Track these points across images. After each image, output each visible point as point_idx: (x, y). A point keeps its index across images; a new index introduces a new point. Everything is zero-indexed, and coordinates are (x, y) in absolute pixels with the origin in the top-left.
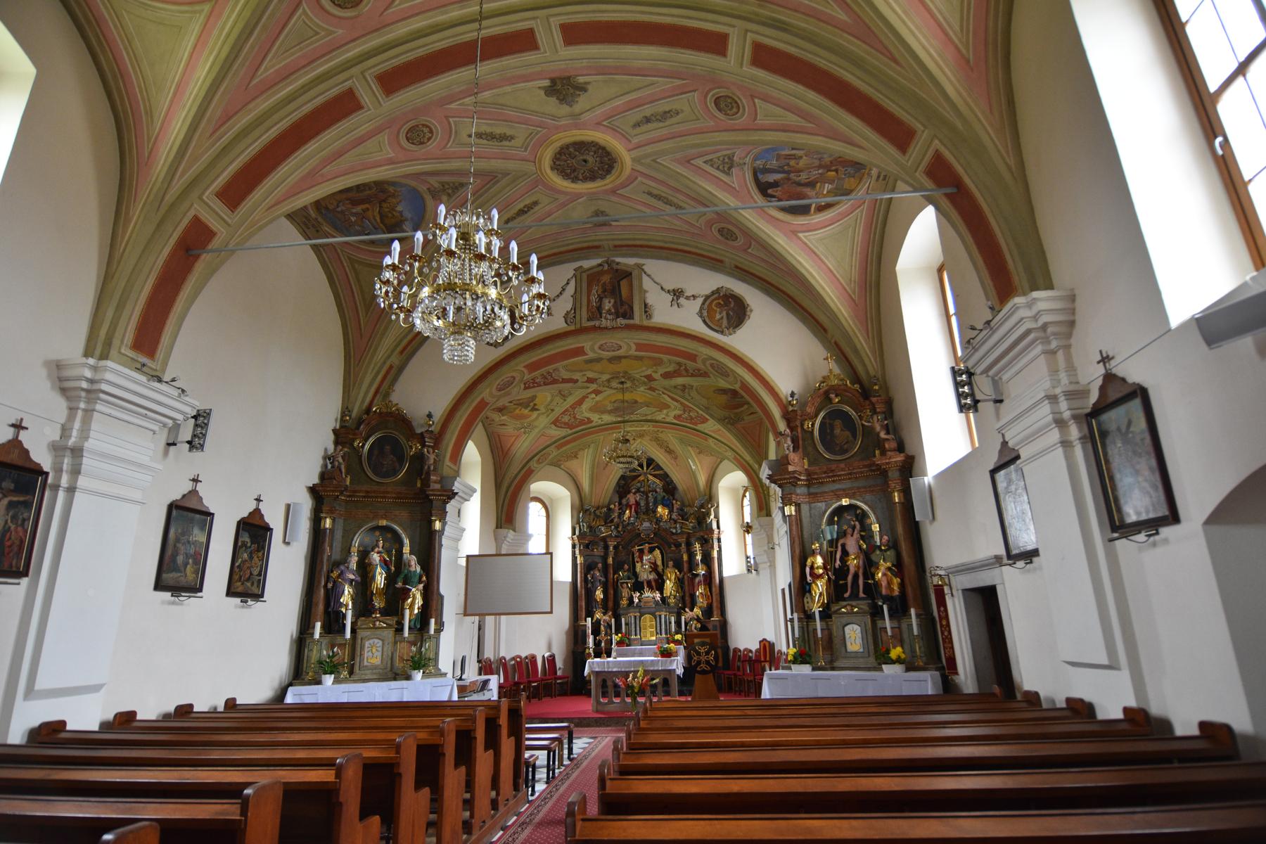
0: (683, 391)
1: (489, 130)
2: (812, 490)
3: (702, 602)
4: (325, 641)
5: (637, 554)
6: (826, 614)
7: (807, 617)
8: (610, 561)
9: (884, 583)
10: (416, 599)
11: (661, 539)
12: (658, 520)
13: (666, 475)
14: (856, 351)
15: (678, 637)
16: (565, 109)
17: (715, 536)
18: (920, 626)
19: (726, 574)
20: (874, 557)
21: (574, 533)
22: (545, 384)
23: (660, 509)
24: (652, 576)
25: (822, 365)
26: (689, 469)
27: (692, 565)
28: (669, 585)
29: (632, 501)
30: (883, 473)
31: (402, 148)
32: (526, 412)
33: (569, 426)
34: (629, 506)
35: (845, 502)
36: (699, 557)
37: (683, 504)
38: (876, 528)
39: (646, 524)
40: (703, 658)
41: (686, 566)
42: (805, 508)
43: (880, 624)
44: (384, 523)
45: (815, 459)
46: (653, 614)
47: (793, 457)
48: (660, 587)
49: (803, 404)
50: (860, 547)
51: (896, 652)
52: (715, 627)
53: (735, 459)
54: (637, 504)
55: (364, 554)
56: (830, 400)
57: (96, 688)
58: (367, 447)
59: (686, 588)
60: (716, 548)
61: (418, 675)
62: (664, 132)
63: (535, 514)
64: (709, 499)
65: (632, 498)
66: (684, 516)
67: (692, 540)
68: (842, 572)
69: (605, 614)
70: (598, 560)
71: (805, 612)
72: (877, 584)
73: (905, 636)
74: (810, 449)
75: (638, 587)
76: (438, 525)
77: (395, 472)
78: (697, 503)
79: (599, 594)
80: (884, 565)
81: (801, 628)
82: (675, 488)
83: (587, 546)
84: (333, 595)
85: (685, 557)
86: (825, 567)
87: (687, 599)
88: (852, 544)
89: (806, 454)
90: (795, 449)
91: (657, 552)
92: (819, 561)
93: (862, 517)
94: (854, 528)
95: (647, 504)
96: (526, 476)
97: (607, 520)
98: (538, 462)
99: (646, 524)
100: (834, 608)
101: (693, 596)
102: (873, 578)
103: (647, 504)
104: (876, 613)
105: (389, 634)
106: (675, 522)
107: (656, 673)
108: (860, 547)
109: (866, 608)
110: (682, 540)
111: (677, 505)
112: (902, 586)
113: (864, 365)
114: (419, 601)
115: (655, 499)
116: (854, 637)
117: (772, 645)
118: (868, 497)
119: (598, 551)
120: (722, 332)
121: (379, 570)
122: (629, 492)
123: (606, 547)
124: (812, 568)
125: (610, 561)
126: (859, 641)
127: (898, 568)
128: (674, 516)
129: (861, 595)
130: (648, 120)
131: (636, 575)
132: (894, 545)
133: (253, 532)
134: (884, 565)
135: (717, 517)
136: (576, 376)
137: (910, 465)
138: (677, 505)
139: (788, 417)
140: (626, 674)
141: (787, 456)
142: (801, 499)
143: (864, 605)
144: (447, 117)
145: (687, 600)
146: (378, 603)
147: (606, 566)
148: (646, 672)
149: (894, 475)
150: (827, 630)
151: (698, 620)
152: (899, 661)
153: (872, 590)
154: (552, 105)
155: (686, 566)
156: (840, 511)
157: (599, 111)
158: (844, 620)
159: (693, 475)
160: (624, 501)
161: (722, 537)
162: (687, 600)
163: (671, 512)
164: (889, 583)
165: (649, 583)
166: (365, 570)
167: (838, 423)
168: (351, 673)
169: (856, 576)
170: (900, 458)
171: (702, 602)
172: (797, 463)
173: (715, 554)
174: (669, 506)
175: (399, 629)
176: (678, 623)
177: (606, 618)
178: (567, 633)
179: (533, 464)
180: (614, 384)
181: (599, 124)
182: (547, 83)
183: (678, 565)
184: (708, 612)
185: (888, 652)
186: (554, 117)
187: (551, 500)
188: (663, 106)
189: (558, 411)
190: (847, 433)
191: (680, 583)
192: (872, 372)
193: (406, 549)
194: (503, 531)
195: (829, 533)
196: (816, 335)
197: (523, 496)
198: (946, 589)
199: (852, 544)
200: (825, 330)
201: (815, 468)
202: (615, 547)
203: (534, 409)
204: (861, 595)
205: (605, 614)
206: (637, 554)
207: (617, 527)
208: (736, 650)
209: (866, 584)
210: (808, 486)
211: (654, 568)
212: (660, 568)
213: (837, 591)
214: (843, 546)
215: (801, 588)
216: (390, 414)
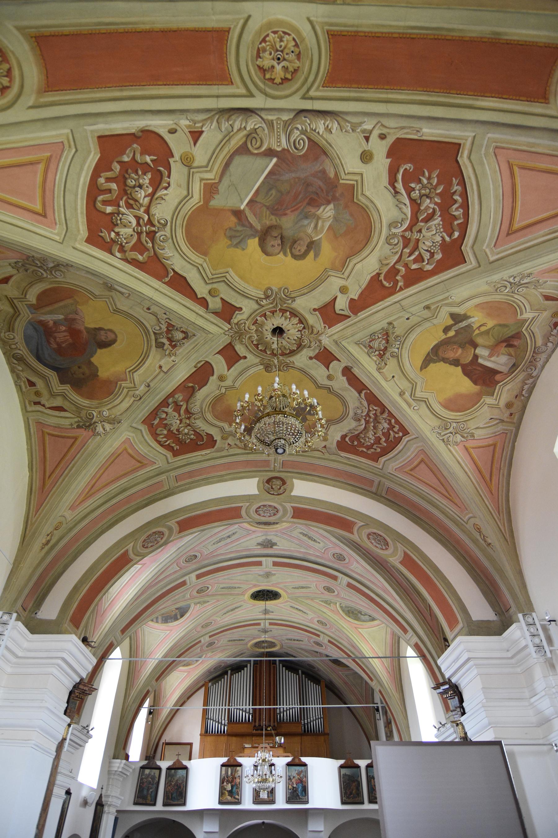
0: (170, 327)
1: (310, 541)
16: (269, 538)
22: (383, 408)
31: (349, 560)
32: (477, 319)
62: (220, 534)
130: (229, 537)
136: (341, 383)
144: (324, 553)
154: (275, 539)
157: (254, 536)
180: (292, 329)
181: (254, 532)
182: (274, 547)
186: (276, 535)
188: (220, 544)
203: (456, 318)
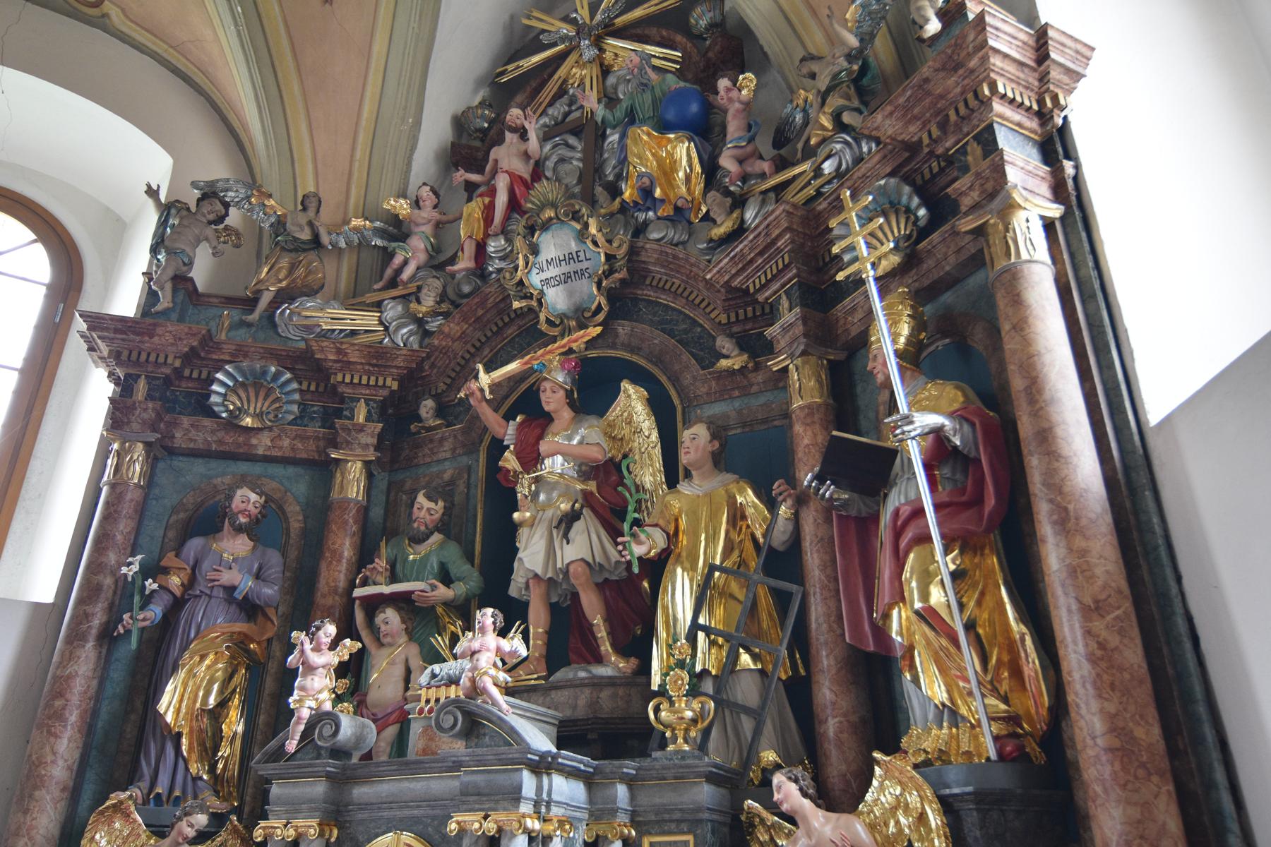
19: (1165, 381)
36: (890, 334)
60: (1032, 209)
87: (829, 693)
91: (632, 402)
101: (877, 673)
106: (739, 202)
122: (500, 140)
125: (352, 482)
147: (321, 510)
161: (1083, 112)
183: (755, 457)
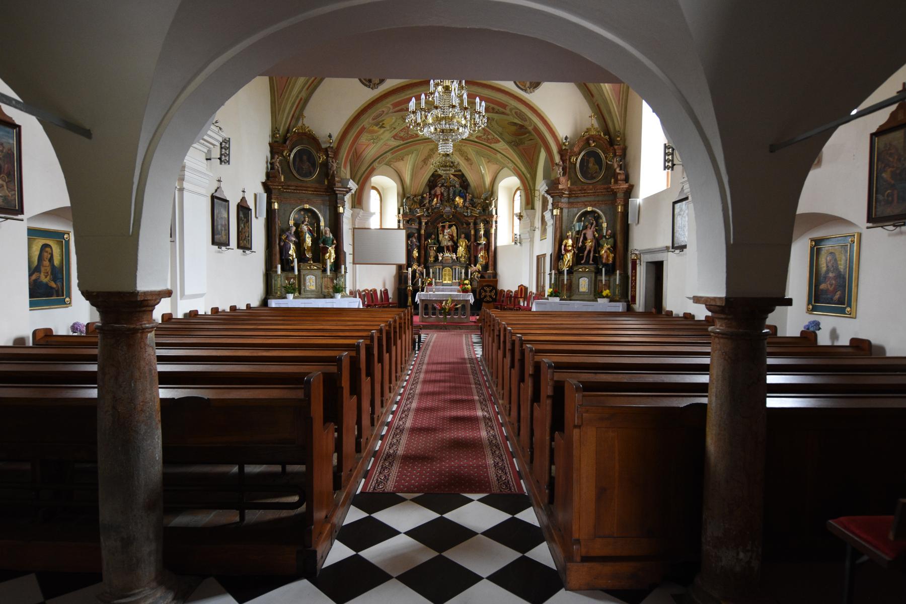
2: (571, 200)
3: (481, 261)
4: (284, 274)
5: (440, 229)
6: (570, 272)
7: (560, 273)
8: (423, 232)
9: (605, 256)
10: (331, 255)
11: (458, 219)
12: (456, 207)
13: (463, 175)
14: (610, 112)
15: (467, 282)
17: (494, 219)
18: (620, 279)
19: (498, 244)
20: (601, 242)
21: (399, 213)
23: (457, 199)
24: (450, 244)
25: (589, 120)
26: (480, 172)
27: (477, 237)
28: (461, 250)
29: (439, 192)
30: (614, 194)
32: (376, 128)
33: (402, 139)
34: (436, 196)
35: (589, 209)
36: (482, 232)
37: (473, 197)
38: (605, 225)
39: (448, 209)
40: (488, 294)
41: (472, 237)
42: (565, 211)
43: (599, 278)
44: (307, 206)
45: (575, 181)
46: (451, 267)
47: (563, 179)
48: (454, 250)
49: (572, 145)
50: (594, 236)
51: (606, 292)
52: (489, 277)
53: (514, 169)
54: (442, 194)
55: (297, 225)
56: (589, 144)
57: (201, 295)
58: (292, 156)
59: (472, 252)
61: (339, 296)
63: (373, 198)
64: (491, 194)
65: (438, 190)
66: (473, 204)
67: (478, 221)
68: (582, 249)
69: (419, 266)
70: (414, 231)
71: (558, 270)
72: (601, 257)
73: (612, 284)
74: (573, 175)
75: (441, 250)
76: (341, 210)
77: (310, 174)
78: (483, 196)
79: (415, 253)
80: (606, 247)
81: (555, 279)
82: (468, 185)
83: (408, 222)
84: (284, 250)
85: (473, 232)
86: (573, 246)
87: (472, 258)
88: (589, 233)
89: (570, 178)
90: (564, 174)
91: (454, 228)
92: (570, 242)
93: (597, 218)
94: (592, 224)
95: (449, 195)
96: (370, 172)
97: (421, 204)
98: (379, 163)
99: (448, 209)
100: (575, 269)
101: (476, 258)
102: (599, 252)
103: (449, 195)
104: (598, 272)
105: (319, 272)
106: (467, 208)
107: (459, 302)
108: (594, 236)
109: (593, 269)
110: (472, 221)
111: (469, 197)
112: (614, 258)
113: (613, 121)
114: (333, 255)
115: (454, 192)
116: (584, 284)
117: (526, 289)
118: (603, 207)
119: (415, 226)
120: (525, 91)
121: (307, 235)
122: (436, 186)
123: (420, 223)
124: (565, 246)
125: (423, 232)
126: (587, 286)
127: (614, 249)
128: (467, 204)
129: (591, 262)
131: (439, 242)
132: (613, 236)
133: (243, 210)
134: (606, 247)
135: (496, 207)
137: (630, 192)
138: (469, 197)
139: (562, 153)
140: (441, 302)
141: (558, 179)
142: (564, 206)
143: (592, 268)
145: (472, 259)
146: (309, 255)
147: (420, 235)
148: (453, 301)
149: (620, 195)
150: (569, 280)
151: (479, 272)
152: (607, 297)
153: (597, 260)
155: (472, 237)
156: (586, 214)
158: (580, 275)
159: (482, 177)
160: (433, 192)
162: (472, 259)
163: (465, 201)
164: (607, 257)
165: (448, 248)
166: (299, 235)
167: (592, 160)
168: (300, 293)
169: (589, 252)
170: (625, 186)
171: (481, 261)
172: (564, 184)
173: (493, 231)
174: (463, 197)
175: (324, 270)
176: (466, 274)
177: (420, 268)
178: (395, 277)
179: (375, 164)
183: (468, 237)
184: (486, 267)
185: (602, 292)
187: (383, 189)
189: (398, 129)
190: (597, 167)
191: (468, 248)
192: (617, 128)
193: (322, 224)
194: (356, 210)
195: (578, 226)
196: (585, 97)
197: (367, 186)
198: (638, 262)
199: (589, 233)
200: (592, 95)
201: (574, 187)
202: (426, 223)
203: (382, 127)
204: (591, 262)
205: (419, 266)
206: (440, 229)
207: (427, 210)
208: (502, 291)
209: (594, 256)
210: (569, 198)
211: (451, 238)
212: (455, 239)
213: (578, 259)
214: (585, 234)
215: (558, 256)
216: (305, 134)
